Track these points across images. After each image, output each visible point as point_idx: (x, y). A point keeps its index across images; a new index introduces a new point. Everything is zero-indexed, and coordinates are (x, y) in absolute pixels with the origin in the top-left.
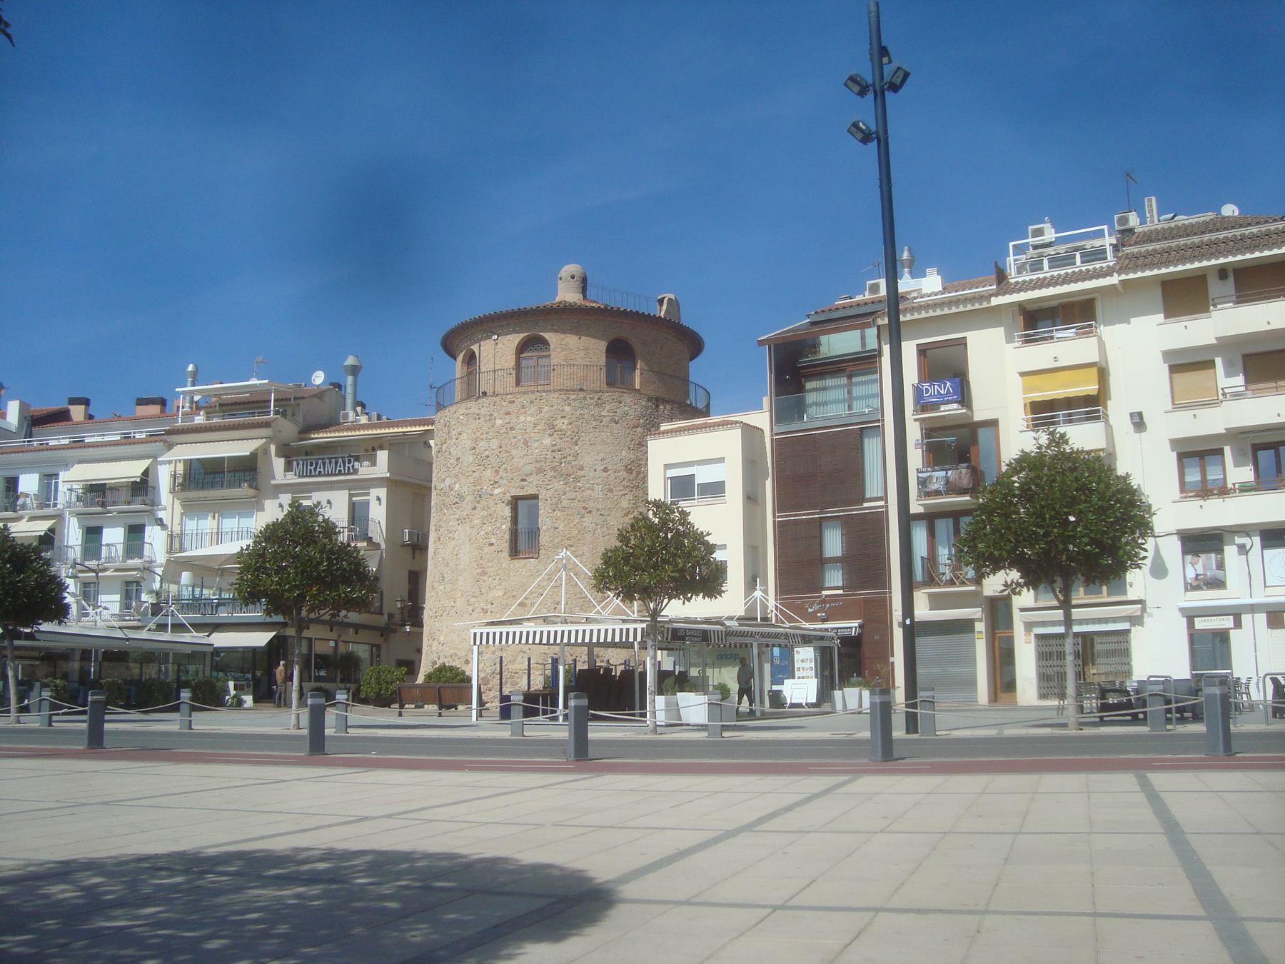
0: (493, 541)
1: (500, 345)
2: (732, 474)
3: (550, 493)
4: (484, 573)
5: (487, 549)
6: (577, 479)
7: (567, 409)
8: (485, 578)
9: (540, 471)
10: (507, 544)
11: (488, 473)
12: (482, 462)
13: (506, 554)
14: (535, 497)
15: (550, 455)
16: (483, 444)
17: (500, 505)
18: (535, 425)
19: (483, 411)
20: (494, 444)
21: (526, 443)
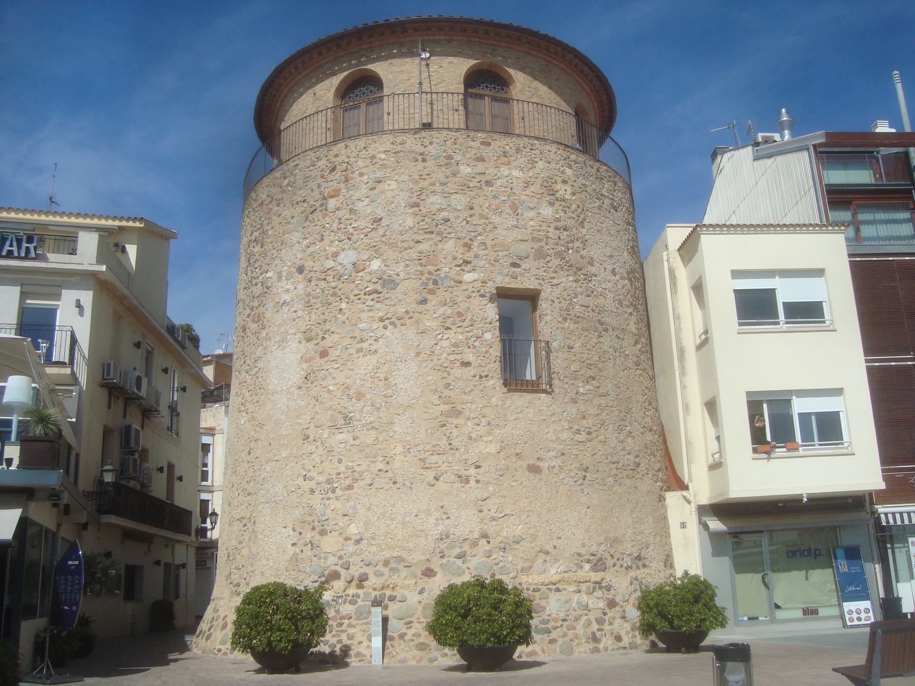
0: (470, 357)
2: (839, 295)
3: (557, 291)
4: (455, 413)
5: (458, 371)
6: (589, 277)
7: (569, 172)
8: (460, 421)
9: (540, 255)
10: (497, 366)
11: (450, 246)
13: (495, 382)
15: (552, 233)
16: (434, 201)
17: (477, 301)
18: (527, 185)
19: (432, 150)
20: (460, 201)
21: (514, 208)
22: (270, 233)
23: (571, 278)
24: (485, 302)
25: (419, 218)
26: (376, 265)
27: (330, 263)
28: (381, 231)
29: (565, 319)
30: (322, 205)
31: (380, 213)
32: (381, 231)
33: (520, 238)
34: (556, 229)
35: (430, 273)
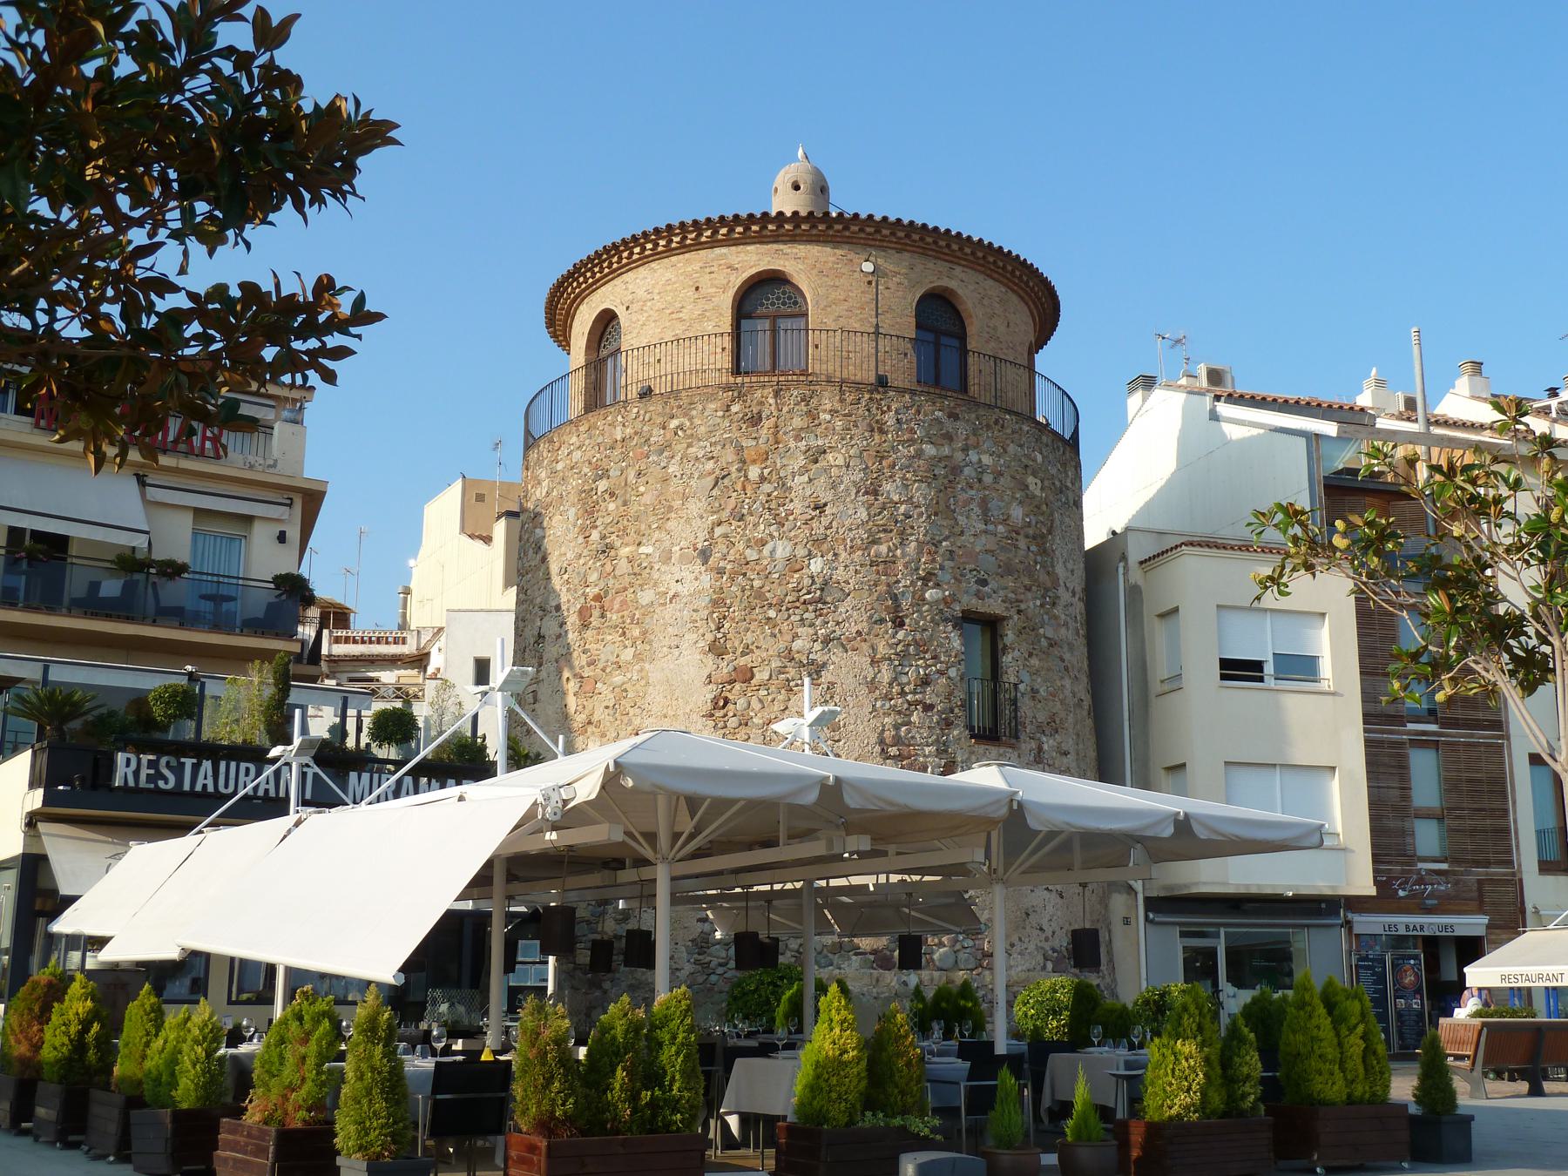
18: (998, 475)
22: (642, 489)
24: (950, 628)
26: (816, 565)
27: (751, 555)
28: (825, 521)
29: (1030, 655)
30: (739, 470)
31: (826, 496)
32: (825, 521)
34: (1027, 536)
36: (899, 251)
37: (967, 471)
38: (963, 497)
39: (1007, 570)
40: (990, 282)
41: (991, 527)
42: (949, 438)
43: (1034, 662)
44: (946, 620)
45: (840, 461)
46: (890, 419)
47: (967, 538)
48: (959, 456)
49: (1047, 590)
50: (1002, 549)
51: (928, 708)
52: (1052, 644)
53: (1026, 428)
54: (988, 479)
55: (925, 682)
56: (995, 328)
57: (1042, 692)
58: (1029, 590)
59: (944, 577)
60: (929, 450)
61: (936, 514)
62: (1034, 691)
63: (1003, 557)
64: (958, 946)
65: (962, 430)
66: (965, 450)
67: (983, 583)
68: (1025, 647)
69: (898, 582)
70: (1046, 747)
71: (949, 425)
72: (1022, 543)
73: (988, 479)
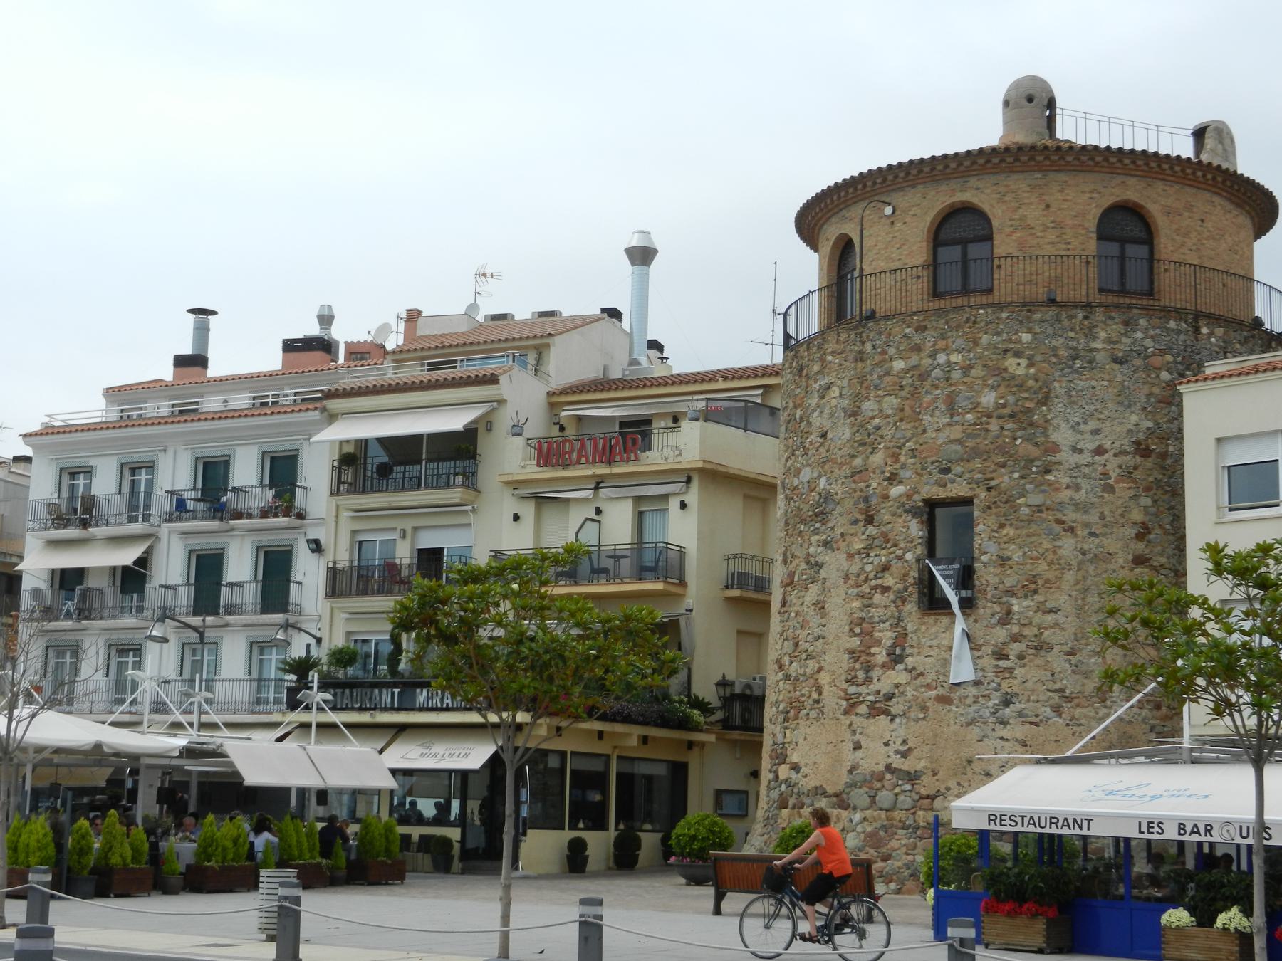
1: (899, 225)
11: (878, 459)
12: (866, 441)
14: (968, 502)
18: (966, 370)
23: (1016, 475)
25: (855, 429)
29: (1002, 526)
33: (952, 437)
34: (999, 417)
35: (861, 490)
36: (914, 186)
37: (934, 374)
38: (928, 398)
39: (975, 453)
40: (1015, 176)
41: (956, 419)
42: (918, 349)
43: (1009, 532)
44: (907, 511)
45: (837, 394)
46: (868, 346)
47: (931, 434)
48: (927, 362)
49: (1031, 461)
50: (969, 436)
51: (886, 589)
52: (1039, 509)
53: (1004, 315)
54: (956, 375)
55: (885, 568)
56: (1023, 218)
57: (1017, 557)
58: (1004, 466)
59: (905, 474)
60: (898, 365)
61: (901, 420)
62: (1003, 560)
63: (971, 444)
64: (897, 790)
65: (929, 340)
66: (933, 356)
67: (947, 471)
68: (992, 521)
69: (868, 486)
70: (1016, 608)
71: (917, 339)
72: (994, 426)
73: (956, 375)
